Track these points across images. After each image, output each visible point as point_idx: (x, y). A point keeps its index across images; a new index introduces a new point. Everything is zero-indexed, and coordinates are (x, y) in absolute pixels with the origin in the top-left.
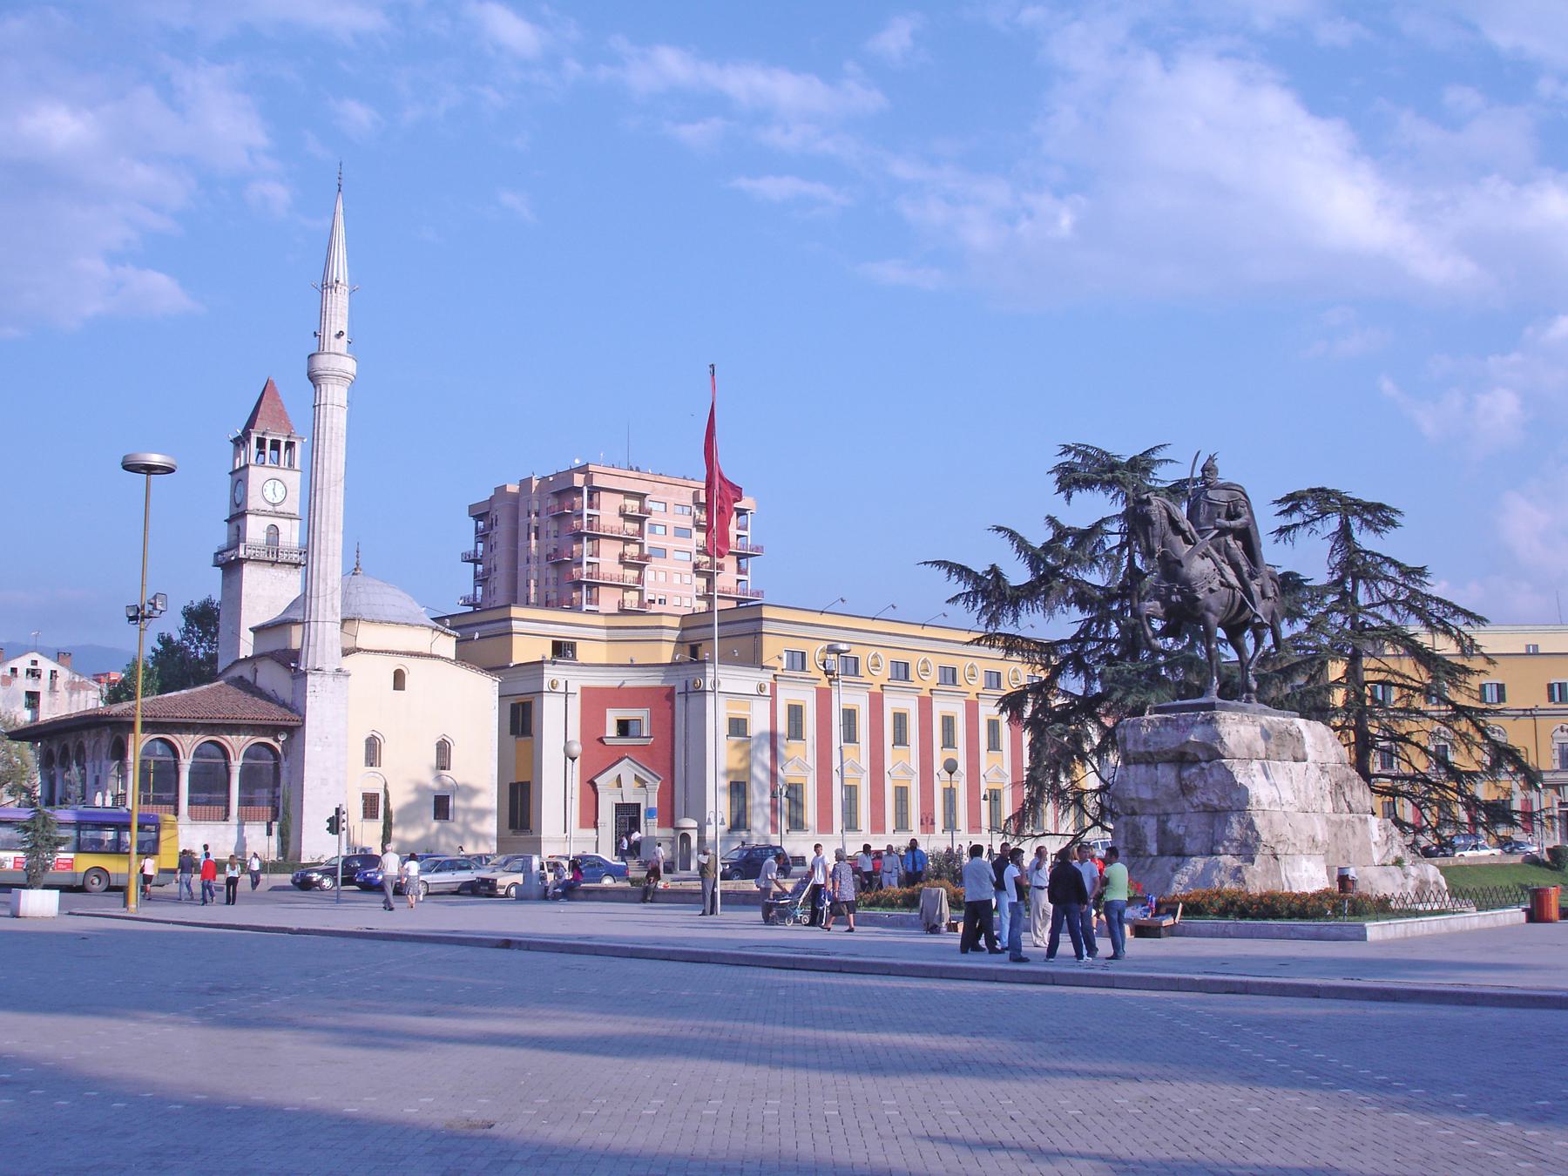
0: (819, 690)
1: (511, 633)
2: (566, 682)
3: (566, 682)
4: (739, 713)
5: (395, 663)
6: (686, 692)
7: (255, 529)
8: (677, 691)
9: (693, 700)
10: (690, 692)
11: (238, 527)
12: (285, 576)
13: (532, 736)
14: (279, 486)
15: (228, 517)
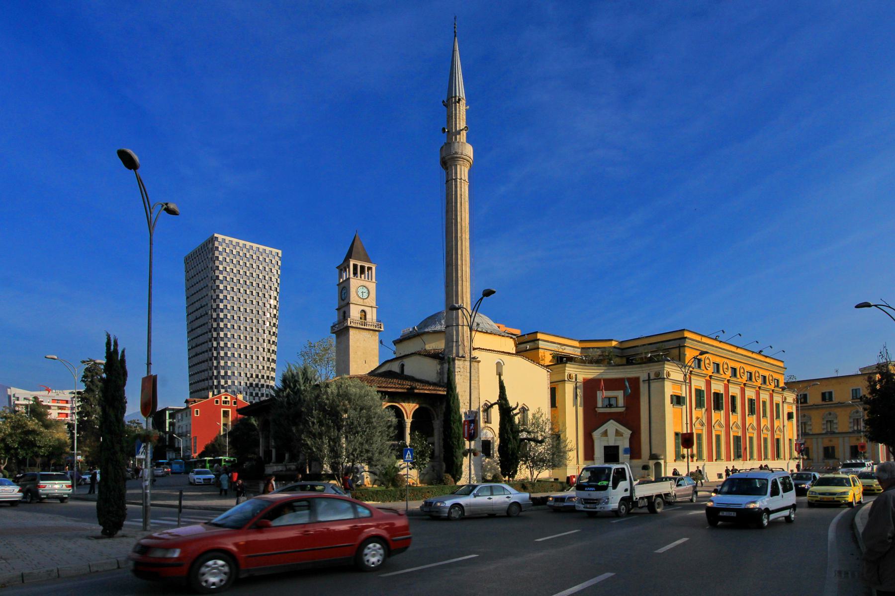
0: (706, 380)
1: (538, 348)
2: (576, 375)
3: (576, 375)
4: (678, 392)
5: (497, 357)
6: (649, 380)
7: (355, 312)
8: (641, 380)
9: (654, 385)
10: (652, 380)
11: (344, 313)
12: (370, 336)
13: (556, 407)
14: (365, 290)
15: (337, 307)
